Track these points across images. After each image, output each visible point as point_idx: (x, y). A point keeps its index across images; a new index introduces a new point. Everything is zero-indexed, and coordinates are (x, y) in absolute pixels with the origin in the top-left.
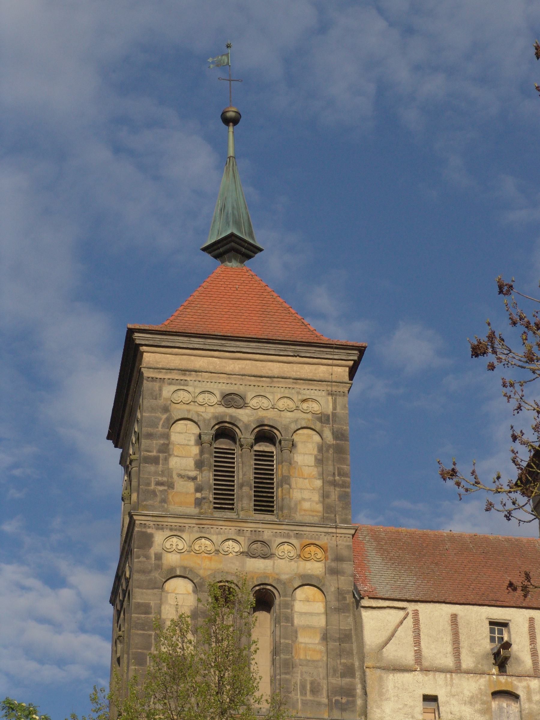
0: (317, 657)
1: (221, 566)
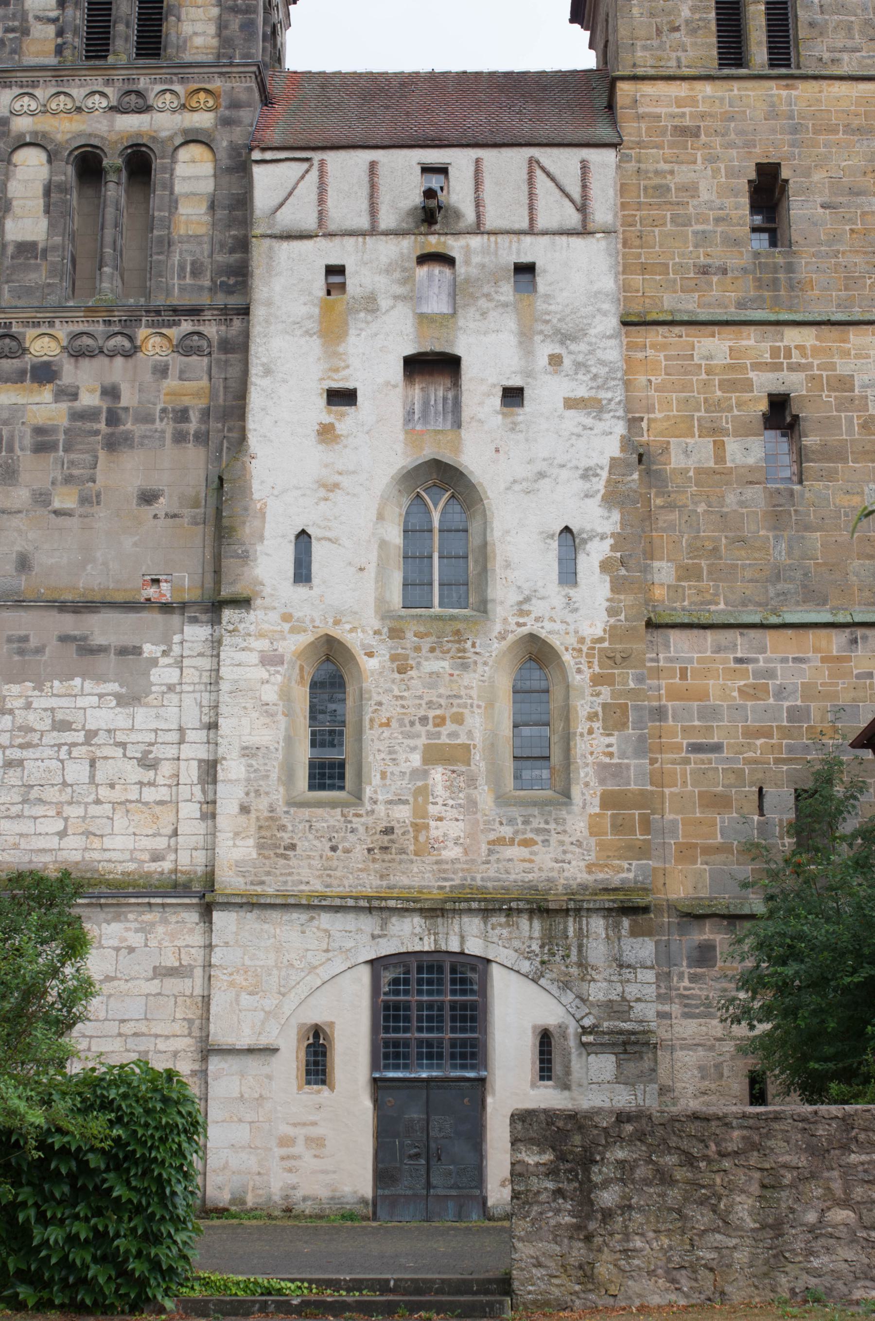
0: (202, 230)
1: (83, 127)
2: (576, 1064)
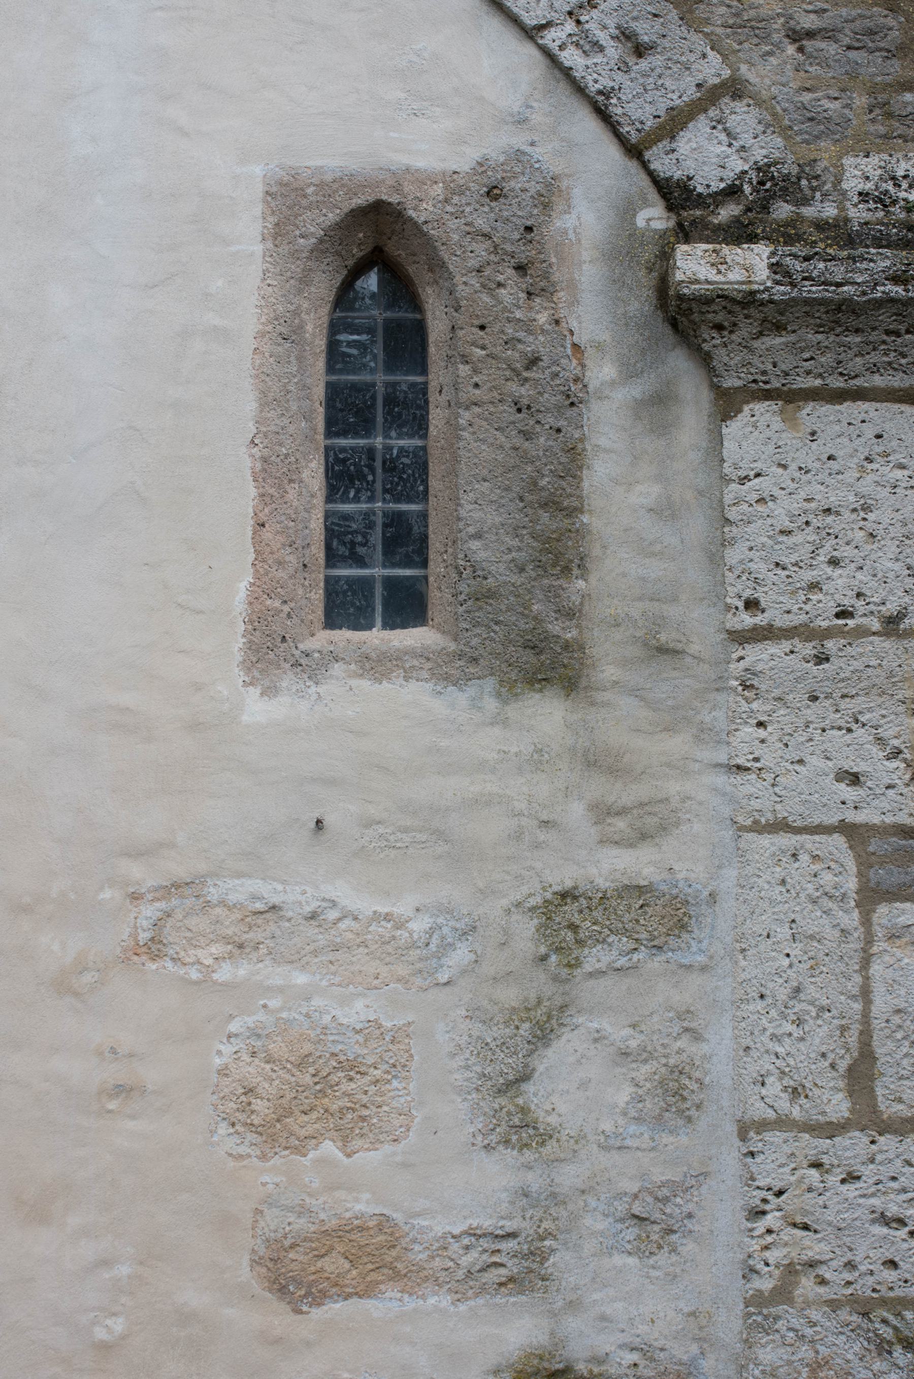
2: (636, 474)
